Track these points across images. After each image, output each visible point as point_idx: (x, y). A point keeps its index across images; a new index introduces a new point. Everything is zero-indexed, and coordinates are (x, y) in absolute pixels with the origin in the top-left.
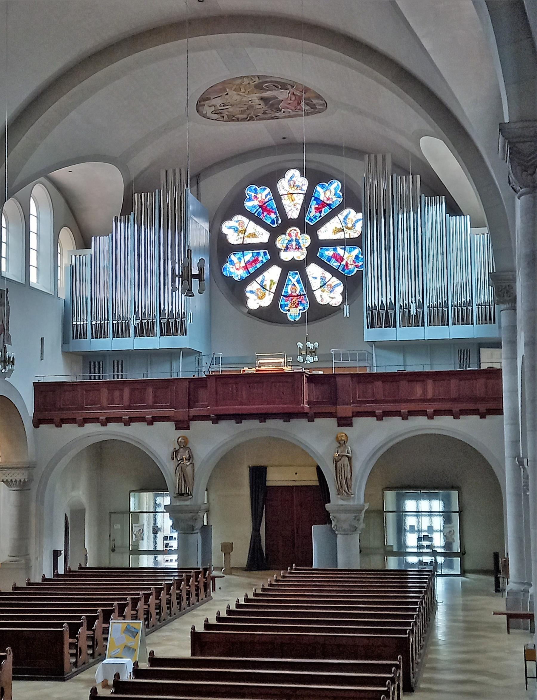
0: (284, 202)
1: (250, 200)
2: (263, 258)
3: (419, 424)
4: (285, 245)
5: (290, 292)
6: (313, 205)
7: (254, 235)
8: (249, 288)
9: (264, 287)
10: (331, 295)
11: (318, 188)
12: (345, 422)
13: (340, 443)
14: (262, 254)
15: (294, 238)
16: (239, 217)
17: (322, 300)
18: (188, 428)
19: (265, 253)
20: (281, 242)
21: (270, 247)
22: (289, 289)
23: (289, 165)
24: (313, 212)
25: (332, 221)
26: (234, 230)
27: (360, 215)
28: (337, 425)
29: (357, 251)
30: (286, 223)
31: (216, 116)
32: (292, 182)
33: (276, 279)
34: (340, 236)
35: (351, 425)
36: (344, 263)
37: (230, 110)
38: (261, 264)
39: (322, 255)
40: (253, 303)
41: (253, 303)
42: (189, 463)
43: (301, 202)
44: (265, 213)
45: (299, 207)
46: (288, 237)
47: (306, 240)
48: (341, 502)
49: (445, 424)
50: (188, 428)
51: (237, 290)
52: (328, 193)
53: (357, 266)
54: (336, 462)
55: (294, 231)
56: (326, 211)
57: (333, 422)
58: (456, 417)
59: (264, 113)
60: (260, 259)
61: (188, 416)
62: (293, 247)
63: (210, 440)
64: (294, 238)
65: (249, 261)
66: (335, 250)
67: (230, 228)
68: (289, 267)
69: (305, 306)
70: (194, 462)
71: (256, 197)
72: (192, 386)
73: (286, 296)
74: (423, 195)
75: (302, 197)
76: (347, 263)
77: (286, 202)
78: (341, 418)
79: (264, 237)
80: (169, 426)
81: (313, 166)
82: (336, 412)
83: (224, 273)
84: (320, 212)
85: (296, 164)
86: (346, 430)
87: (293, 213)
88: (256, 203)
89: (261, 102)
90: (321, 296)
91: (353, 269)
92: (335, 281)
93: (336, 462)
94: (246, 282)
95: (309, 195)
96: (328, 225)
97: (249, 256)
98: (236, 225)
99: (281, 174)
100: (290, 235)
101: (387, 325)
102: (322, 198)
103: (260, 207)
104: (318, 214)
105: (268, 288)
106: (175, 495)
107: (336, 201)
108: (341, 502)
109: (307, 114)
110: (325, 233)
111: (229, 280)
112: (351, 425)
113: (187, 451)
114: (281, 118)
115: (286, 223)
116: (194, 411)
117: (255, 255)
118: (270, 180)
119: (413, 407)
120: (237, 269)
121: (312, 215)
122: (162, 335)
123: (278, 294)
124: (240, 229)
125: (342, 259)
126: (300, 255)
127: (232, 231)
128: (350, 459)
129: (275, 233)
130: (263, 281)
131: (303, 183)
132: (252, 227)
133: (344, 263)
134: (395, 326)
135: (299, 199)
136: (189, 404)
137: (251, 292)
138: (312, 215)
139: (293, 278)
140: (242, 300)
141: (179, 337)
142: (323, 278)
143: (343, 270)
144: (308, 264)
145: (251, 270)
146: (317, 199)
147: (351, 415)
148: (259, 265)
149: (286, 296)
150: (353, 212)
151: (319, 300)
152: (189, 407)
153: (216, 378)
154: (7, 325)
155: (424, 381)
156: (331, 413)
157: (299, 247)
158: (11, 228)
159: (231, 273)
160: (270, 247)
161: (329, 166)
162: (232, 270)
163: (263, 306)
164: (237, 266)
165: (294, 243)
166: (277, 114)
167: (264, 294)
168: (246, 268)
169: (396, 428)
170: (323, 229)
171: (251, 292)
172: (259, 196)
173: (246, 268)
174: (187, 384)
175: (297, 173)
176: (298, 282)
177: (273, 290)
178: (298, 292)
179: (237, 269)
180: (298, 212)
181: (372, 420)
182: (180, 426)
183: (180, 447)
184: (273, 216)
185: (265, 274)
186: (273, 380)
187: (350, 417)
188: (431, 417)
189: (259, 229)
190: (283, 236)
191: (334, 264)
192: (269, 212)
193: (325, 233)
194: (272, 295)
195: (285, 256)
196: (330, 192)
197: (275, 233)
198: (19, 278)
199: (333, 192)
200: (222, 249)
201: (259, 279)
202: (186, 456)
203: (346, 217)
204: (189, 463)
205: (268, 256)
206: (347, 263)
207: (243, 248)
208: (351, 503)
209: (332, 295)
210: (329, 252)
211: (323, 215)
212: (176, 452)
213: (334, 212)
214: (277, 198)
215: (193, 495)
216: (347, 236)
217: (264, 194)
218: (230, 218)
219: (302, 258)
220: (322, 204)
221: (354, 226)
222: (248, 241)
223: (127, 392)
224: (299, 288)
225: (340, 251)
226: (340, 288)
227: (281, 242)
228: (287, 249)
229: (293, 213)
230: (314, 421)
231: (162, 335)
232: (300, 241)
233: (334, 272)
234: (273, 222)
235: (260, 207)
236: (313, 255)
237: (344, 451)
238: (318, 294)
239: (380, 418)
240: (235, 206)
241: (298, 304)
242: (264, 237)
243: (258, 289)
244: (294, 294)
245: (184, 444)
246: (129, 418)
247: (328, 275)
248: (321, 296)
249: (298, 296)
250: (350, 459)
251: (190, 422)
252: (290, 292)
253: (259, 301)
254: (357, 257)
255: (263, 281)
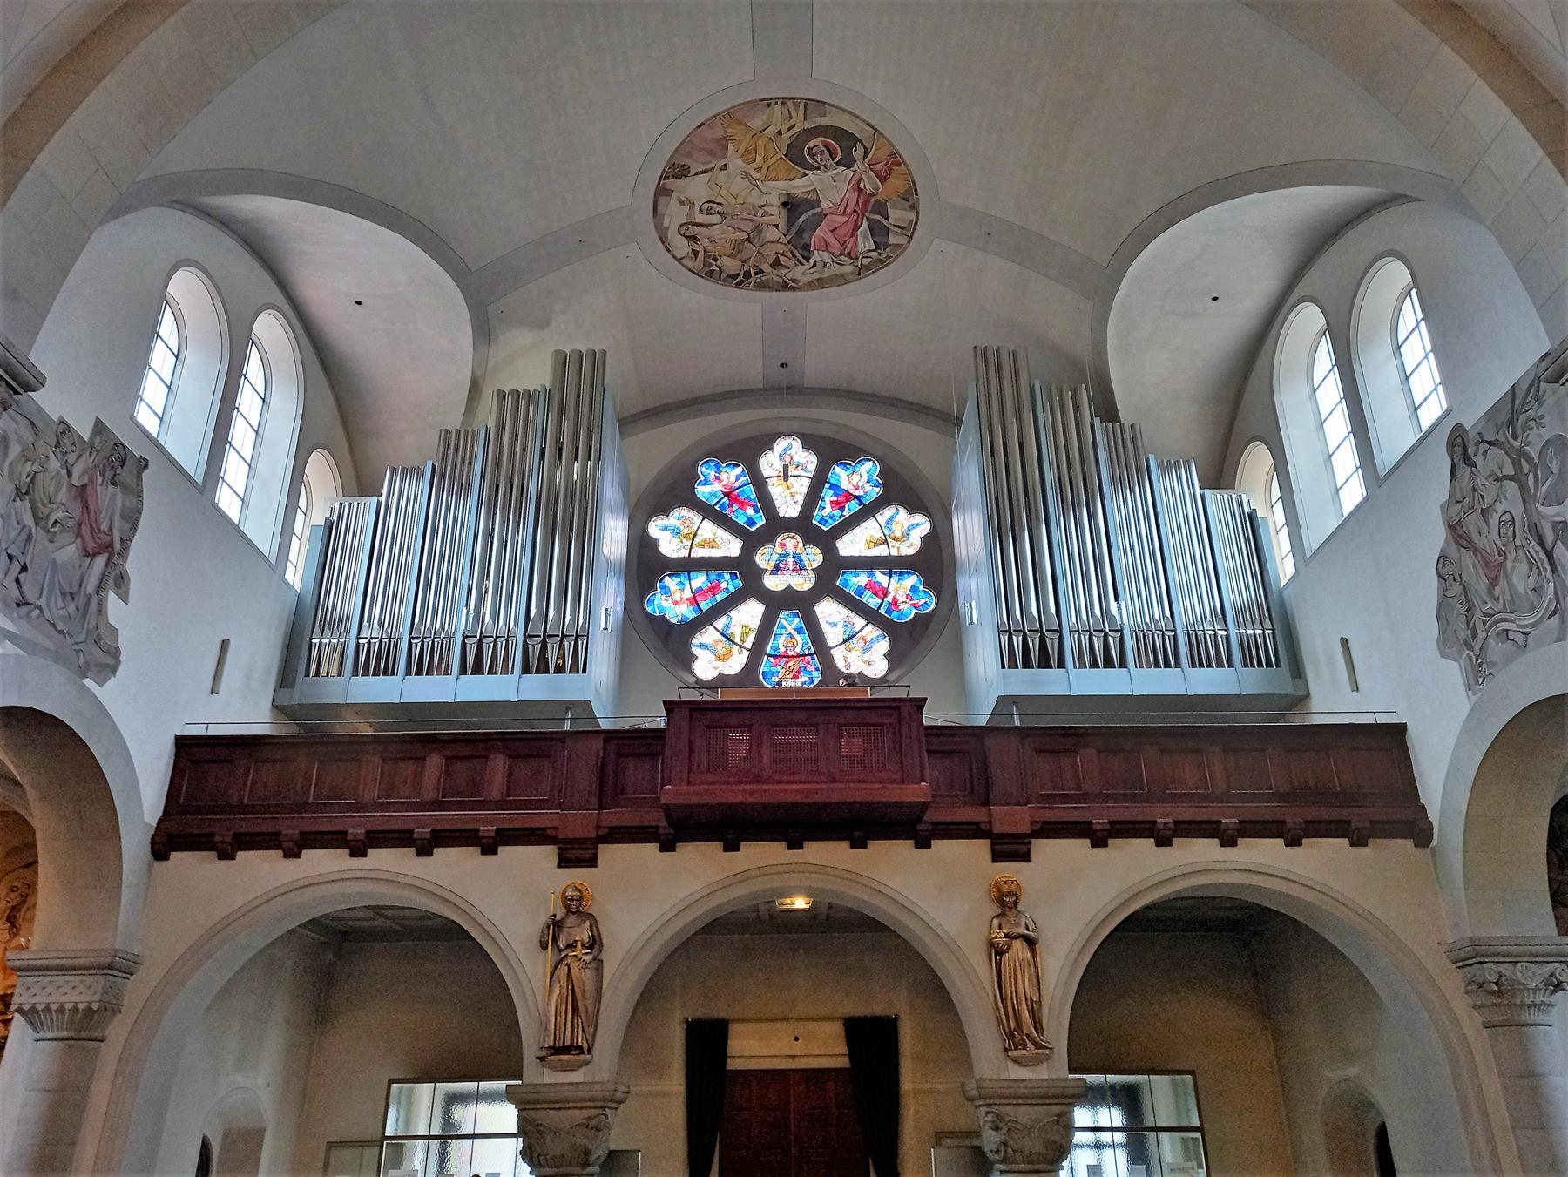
0: (772, 489)
1: (706, 483)
2: (729, 584)
3: (1196, 863)
4: (772, 563)
5: (782, 649)
6: (828, 495)
7: (712, 544)
8: (697, 640)
9: (729, 639)
10: (865, 657)
11: (838, 469)
12: (1011, 849)
13: (1003, 904)
14: (727, 577)
15: (791, 551)
16: (686, 512)
17: (848, 665)
18: (592, 862)
19: (733, 576)
20: (763, 558)
21: (743, 566)
22: (779, 643)
23: (783, 427)
24: (826, 510)
25: (864, 525)
26: (670, 535)
27: (920, 518)
28: (988, 856)
29: (912, 580)
30: (776, 525)
31: (682, 246)
32: (787, 458)
33: (755, 623)
34: (881, 551)
35: (1026, 857)
36: (889, 599)
37: (715, 232)
38: (725, 595)
39: (846, 584)
40: (705, 668)
41: (705, 668)
42: (589, 958)
43: (804, 490)
44: (735, 507)
45: (801, 499)
46: (778, 550)
47: (814, 557)
48: (1016, 1072)
49: (1261, 865)
50: (592, 862)
51: (674, 642)
52: (855, 478)
53: (915, 606)
54: (997, 951)
55: (791, 543)
56: (852, 507)
57: (982, 847)
58: (1294, 842)
59: (776, 264)
60: (724, 585)
61: (598, 827)
62: (789, 566)
63: (652, 894)
64: (791, 551)
65: (700, 589)
66: (871, 575)
67: (665, 528)
68: (777, 603)
69: (815, 674)
70: (603, 956)
71: (717, 478)
72: (612, 747)
73: (775, 657)
74: (1097, 421)
75: (807, 482)
76: (894, 599)
77: (776, 490)
78: (1003, 836)
79: (731, 547)
80: (546, 855)
81: (827, 432)
82: (990, 822)
83: (649, 609)
84: (842, 509)
85: (796, 425)
86: (1009, 871)
87: (789, 508)
88: (717, 488)
89: (778, 215)
90: (846, 659)
91: (907, 612)
92: (871, 631)
93: (1000, 953)
94: (693, 626)
95: (819, 481)
96: (856, 531)
97: (700, 580)
98: (678, 523)
99: (767, 442)
100: (783, 546)
101: (1045, 663)
102: (845, 484)
103: (726, 495)
104: (837, 512)
105: (737, 640)
106: (544, 1053)
107: (873, 493)
108: (1016, 1072)
109: (860, 272)
110: (851, 545)
111: (660, 625)
112: (1026, 857)
113: (587, 924)
114: (800, 289)
115: (776, 525)
116: (617, 817)
117: (713, 578)
118: (746, 451)
119: (1187, 813)
120: (676, 603)
121: (825, 513)
122: (526, 670)
123: (757, 652)
124: (685, 531)
125: (885, 593)
126: (803, 583)
127: (668, 534)
128: (1031, 943)
129: (753, 540)
130: (727, 626)
131: (810, 461)
132: (708, 529)
133: (889, 599)
134: (1061, 665)
135: (801, 486)
136: (600, 800)
137: (703, 646)
138: (825, 513)
139: (789, 623)
140: (687, 660)
141: (566, 677)
142: (847, 625)
143: (889, 611)
144: (819, 599)
145: (705, 606)
146: (833, 486)
147: (1026, 829)
148: (719, 598)
149: (775, 657)
150: (903, 513)
151: (841, 665)
152: (601, 808)
153: (691, 710)
154: (126, 542)
155: (1201, 751)
156: (977, 823)
157: (800, 568)
158: (190, 358)
159: (661, 609)
160: (743, 566)
161: (859, 431)
162: (665, 604)
163: (726, 672)
164: (677, 597)
165: (791, 560)
166: (800, 272)
167: (730, 653)
168: (694, 601)
169: (1137, 871)
170: (846, 538)
171: (703, 646)
172: (724, 476)
173: (694, 601)
174: (598, 744)
175: (797, 444)
176: (799, 631)
177: (749, 644)
178: (798, 649)
179: (676, 603)
180: (799, 508)
181: (1081, 846)
182: (571, 854)
183: (569, 912)
184: (750, 511)
185: (733, 613)
186: (842, 721)
187: (1024, 836)
188: (1229, 841)
189: (722, 534)
190: (769, 548)
191: (873, 602)
192: (743, 505)
193: (851, 545)
194: (746, 653)
195: (773, 583)
196: (860, 478)
197: (753, 540)
198: (188, 451)
199: (865, 477)
200: (646, 567)
201: (720, 623)
202: (583, 934)
203: (891, 519)
204: (589, 958)
205: (739, 582)
206: (894, 599)
207: (688, 565)
208: (1042, 1072)
209: (867, 657)
210: (861, 579)
211: (846, 513)
212: (557, 925)
213: (869, 511)
214: (759, 482)
215: (595, 1051)
216: (894, 553)
217: (733, 475)
218: (665, 511)
219: (807, 586)
220: (844, 497)
221: (906, 535)
222: (698, 553)
223: (434, 763)
224: (802, 642)
225: (881, 578)
226: (884, 645)
227: (763, 558)
228: (777, 569)
229: (789, 508)
230: (929, 846)
231: (526, 670)
232: (803, 557)
233: (871, 616)
234: (751, 522)
235: (726, 495)
236: (827, 584)
237: (1018, 925)
238: (838, 655)
239: (1099, 842)
240: (674, 491)
241: (799, 672)
242: (731, 547)
243: (716, 642)
244: (790, 653)
245: (576, 906)
246: (433, 831)
247: (859, 622)
248: (846, 659)
249: (798, 656)
250: (1031, 943)
251: (601, 846)
252: (782, 649)
253: (719, 664)
254: (914, 589)
255: (727, 626)
